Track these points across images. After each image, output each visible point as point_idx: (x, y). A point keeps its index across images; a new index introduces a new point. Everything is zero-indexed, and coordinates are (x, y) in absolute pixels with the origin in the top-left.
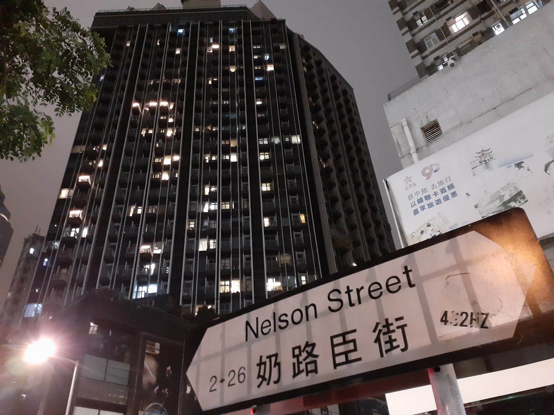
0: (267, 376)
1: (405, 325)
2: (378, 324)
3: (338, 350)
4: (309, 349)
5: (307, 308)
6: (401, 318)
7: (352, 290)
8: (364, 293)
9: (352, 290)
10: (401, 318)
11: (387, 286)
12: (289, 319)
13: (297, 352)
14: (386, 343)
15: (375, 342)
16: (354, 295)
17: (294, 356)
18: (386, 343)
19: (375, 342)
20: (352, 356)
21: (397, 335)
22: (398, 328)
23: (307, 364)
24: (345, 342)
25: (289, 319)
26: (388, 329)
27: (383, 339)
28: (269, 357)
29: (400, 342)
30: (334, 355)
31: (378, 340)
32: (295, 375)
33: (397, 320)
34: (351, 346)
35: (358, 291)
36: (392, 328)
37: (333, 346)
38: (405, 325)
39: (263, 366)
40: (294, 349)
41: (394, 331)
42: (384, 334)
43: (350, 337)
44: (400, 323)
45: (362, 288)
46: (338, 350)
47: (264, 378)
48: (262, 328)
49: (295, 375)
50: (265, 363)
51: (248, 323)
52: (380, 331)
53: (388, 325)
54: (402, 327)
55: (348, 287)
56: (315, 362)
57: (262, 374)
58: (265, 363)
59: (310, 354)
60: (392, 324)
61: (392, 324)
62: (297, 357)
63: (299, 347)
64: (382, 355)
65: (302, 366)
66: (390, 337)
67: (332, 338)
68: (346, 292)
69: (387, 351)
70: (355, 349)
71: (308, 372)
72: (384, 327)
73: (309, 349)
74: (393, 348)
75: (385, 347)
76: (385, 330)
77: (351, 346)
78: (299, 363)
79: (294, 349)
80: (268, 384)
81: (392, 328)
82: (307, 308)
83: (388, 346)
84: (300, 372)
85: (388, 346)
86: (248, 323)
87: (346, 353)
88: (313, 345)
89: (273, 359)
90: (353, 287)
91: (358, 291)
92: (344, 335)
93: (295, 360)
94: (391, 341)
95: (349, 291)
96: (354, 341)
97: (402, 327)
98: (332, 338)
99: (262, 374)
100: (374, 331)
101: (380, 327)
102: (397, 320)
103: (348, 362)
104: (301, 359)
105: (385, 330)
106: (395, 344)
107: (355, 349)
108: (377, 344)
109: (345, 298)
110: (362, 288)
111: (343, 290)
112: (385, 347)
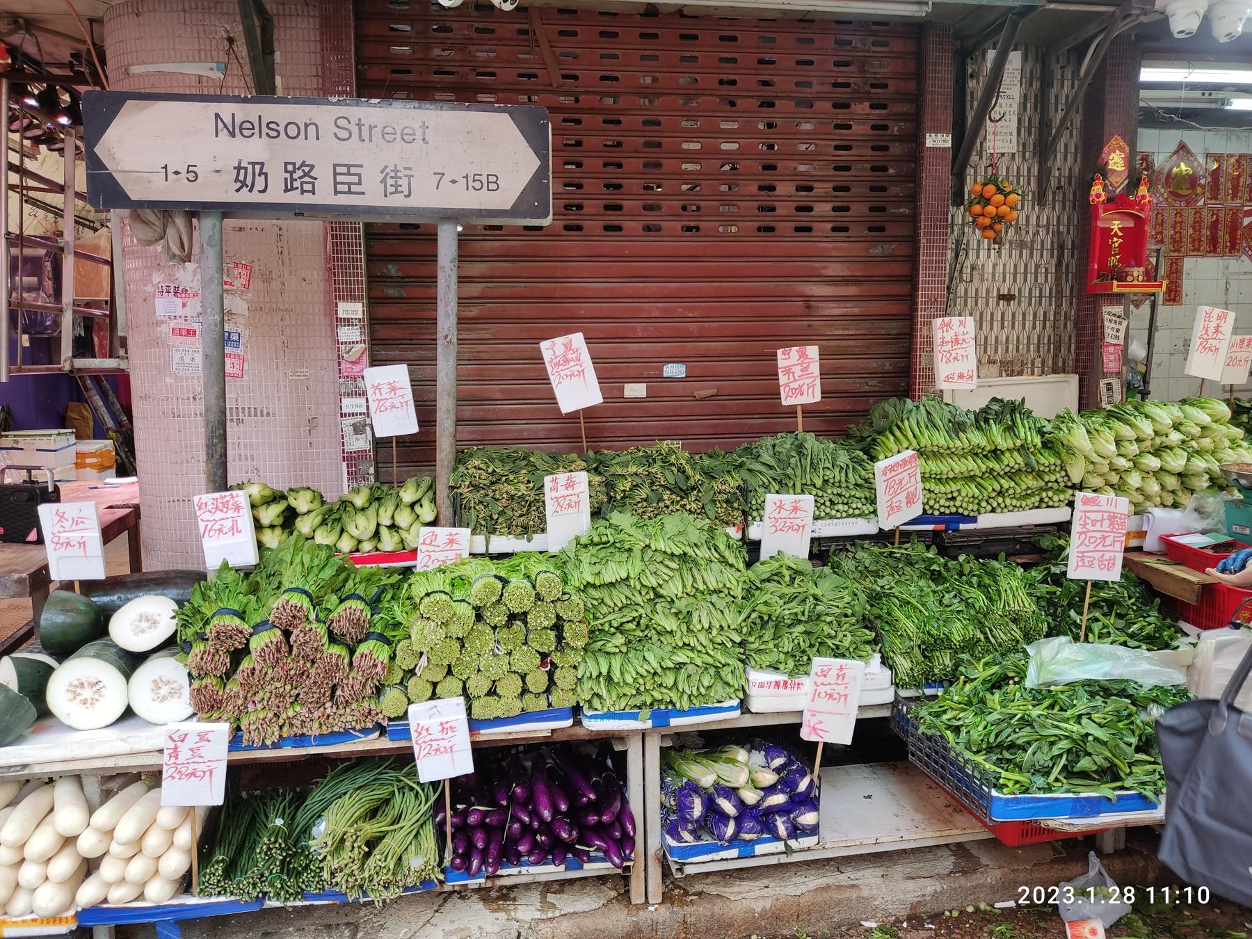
0: (249, 182)
2: (386, 167)
3: (339, 179)
4: (307, 169)
5: (306, 126)
12: (281, 129)
13: (290, 168)
16: (365, 130)
17: (286, 171)
20: (354, 188)
21: (404, 182)
23: (302, 183)
24: (349, 174)
25: (281, 129)
27: (390, 182)
28: (253, 164)
29: (405, 189)
30: (336, 183)
31: (384, 181)
32: (286, 190)
34: (355, 179)
37: (335, 174)
39: (242, 171)
40: (286, 164)
43: (353, 170)
46: (339, 179)
47: (244, 184)
48: (241, 129)
49: (286, 190)
50: (246, 169)
51: (217, 115)
53: (396, 171)
54: (410, 177)
56: (313, 184)
57: (242, 178)
58: (246, 169)
59: (306, 174)
62: (291, 173)
63: (294, 164)
65: (297, 184)
67: (335, 166)
70: (360, 183)
71: (303, 192)
73: (307, 169)
74: (397, 192)
75: (390, 189)
76: (393, 174)
77: (355, 179)
78: (293, 180)
79: (286, 164)
80: (250, 191)
82: (306, 126)
83: (393, 189)
84: (293, 189)
85: (393, 189)
86: (217, 115)
87: (349, 184)
88: (312, 167)
89: (257, 167)
91: (371, 128)
92: (349, 166)
93: (288, 175)
94: (396, 186)
95: (359, 125)
96: (359, 175)
97: (410, 177)
98: (335, 166)
99: (242, 178)
100: (382, 172)
101: (388, 170)
103: (350, 192)
104: (295, 176)
107: (360, 183)
109: (355, 129)
111: (354, 121)
112: (390, 189)
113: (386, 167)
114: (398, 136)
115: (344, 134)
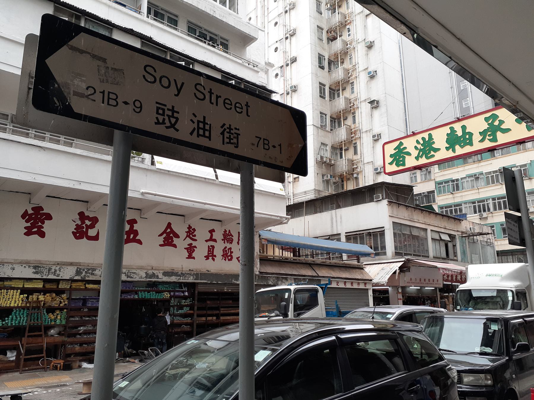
1: (239, 135)
2: (224, 125)
6: (238, 130)
7: (213, 93)
8: (221, 101)
9: (213, 93)
10: (238, 130)
11: (235, 107)
14: (227, 138)
15: (221, 134)
18: (227, 138)
19: (221, 134)
22: (235, 133)
26: (230, 131)
31: (223, 133)
33: (236, 129)
35: (218, 97)
36: (232, 131)
38: (239, 135)
41: (232, 134)
42: (228, 132)
44: (237, 131)
45: (220, 97)
52: (225, 129)
53: (230, 128)
54: (238, 134)
55: (211, 89)
60: (232, 129)
61: (232, 129)
64: (223, 144)
66: (230, 136)
68: (209, 92)
69: (228, 143)
72: (228, 128)
74: (229, 143)
75: (227, 140)
76: (228, 130)
81: (232, 131)
83: (228, 140)
85: (228, 140)
90: (216, 92)
91: (218, 97)
95: (211, 93)
97: (238, 134)
100: (222, 127)
101: (225, 127)
102: (236, 129)
105: (228, 130)
106: (232, 141)
108: (222, 136)
110: (220, 97)
113: (224, 125)
114: (233, 107)
115: (202, 97)
